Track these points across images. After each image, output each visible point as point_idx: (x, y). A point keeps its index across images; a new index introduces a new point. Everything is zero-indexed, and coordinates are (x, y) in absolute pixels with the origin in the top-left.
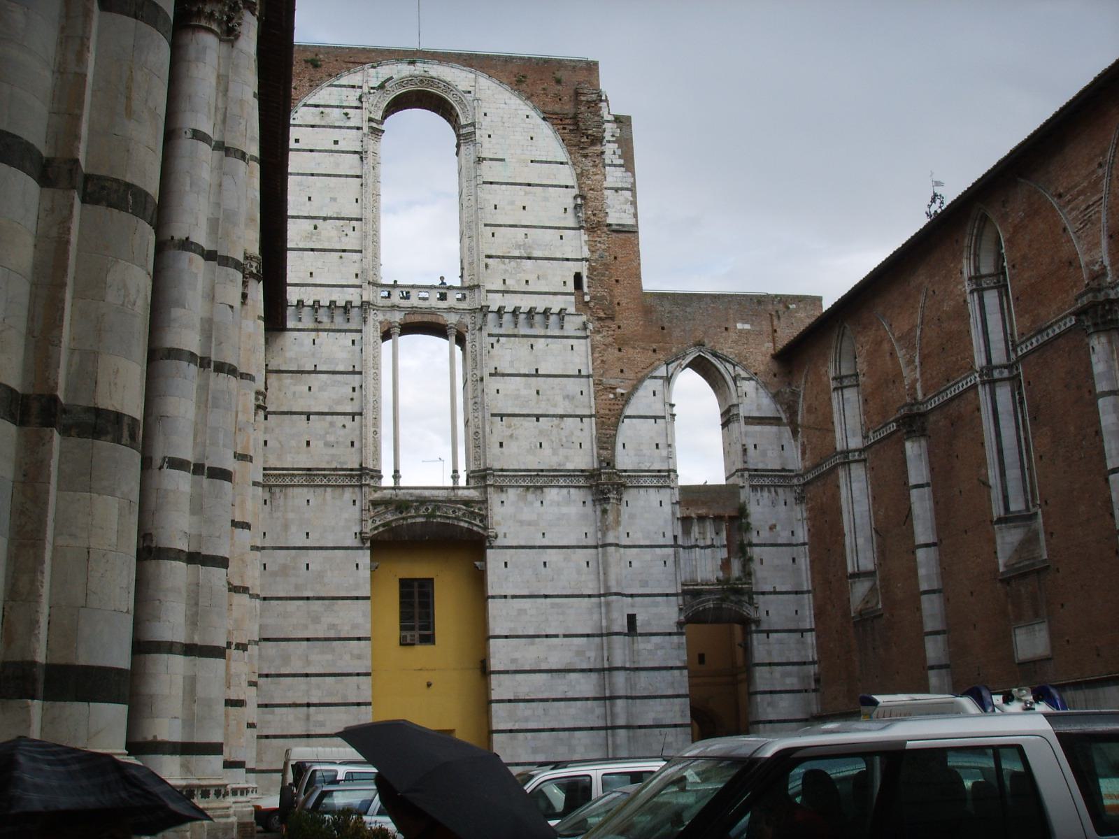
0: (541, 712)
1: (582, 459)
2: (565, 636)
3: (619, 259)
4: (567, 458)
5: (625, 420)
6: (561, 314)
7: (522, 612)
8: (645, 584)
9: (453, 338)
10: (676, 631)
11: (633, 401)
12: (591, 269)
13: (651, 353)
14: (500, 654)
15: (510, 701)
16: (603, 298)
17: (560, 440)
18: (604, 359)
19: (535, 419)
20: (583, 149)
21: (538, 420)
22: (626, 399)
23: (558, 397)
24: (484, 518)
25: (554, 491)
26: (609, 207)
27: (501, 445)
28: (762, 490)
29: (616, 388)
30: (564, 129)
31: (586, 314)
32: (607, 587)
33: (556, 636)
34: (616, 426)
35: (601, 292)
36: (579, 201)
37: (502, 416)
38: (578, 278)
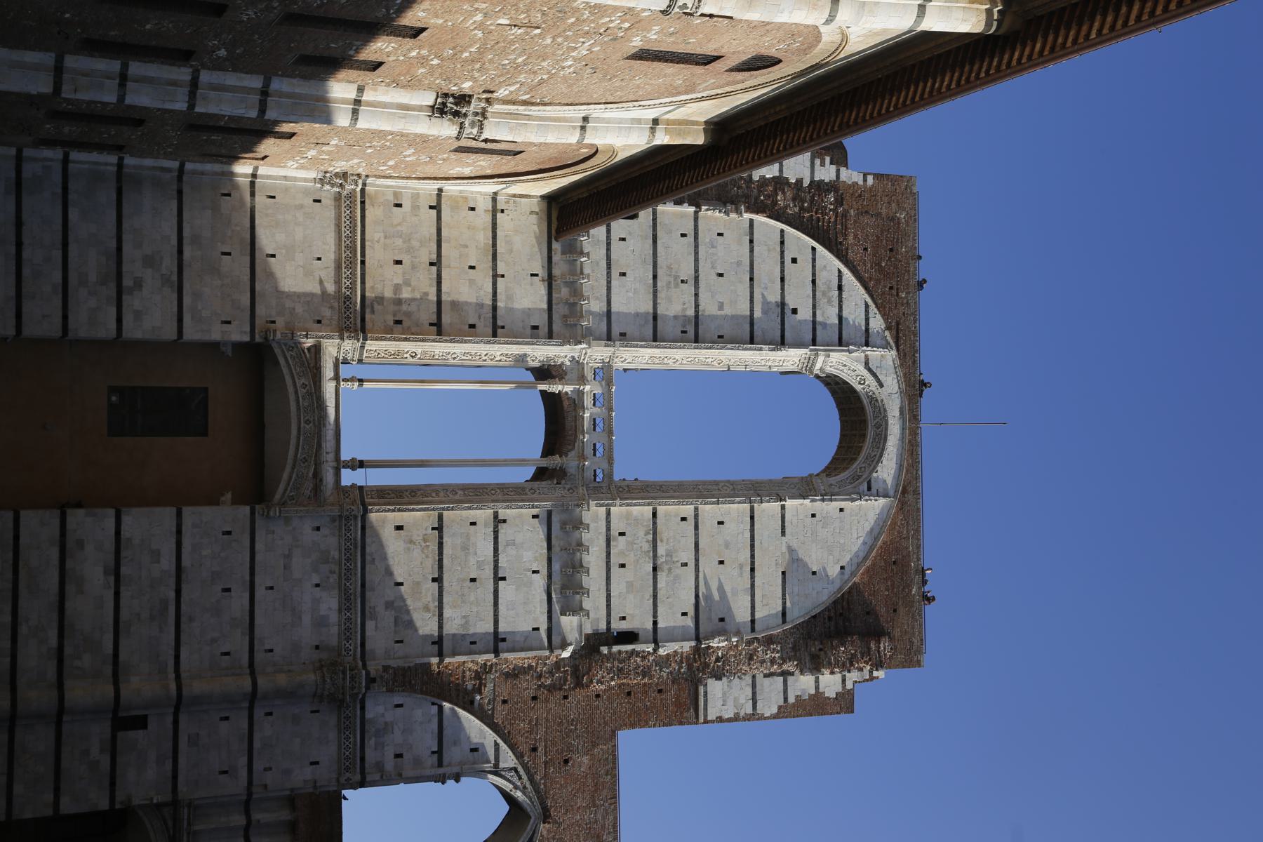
5: (437, 706)
9: (544, 463)
19: (436, 576)
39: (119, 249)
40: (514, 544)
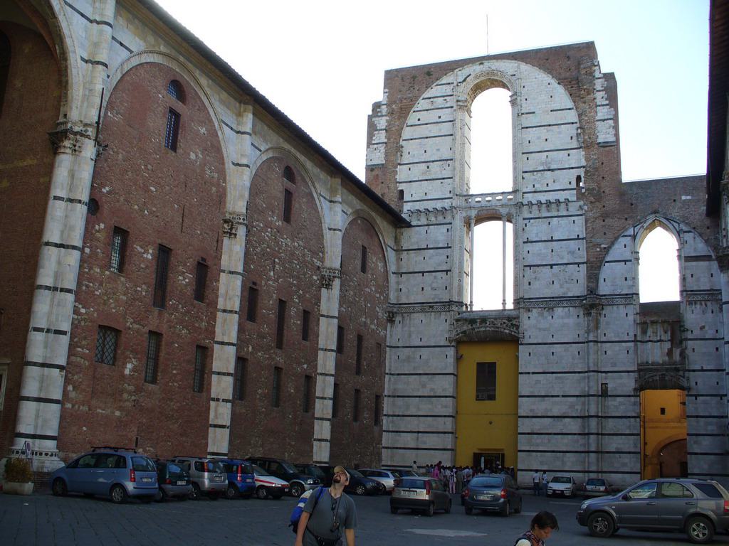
0: (546, 441)
1: (578, 289)
2: (563, 396)
3: (605, 164)
4: (568, 289)
6: (567, 201)
7: (538, 382)
8: (614, 365)
10: (633, 394)
11: (611, 252)
12: (586, 172)
13: (624, 221)
14: (525, 406)
15: (528, 434)
16: (593, 189)
17: (565, 278)
18: (594, 227)
20: (583, 98)
21: (552, 268)
22: (607, 250)
23: (563, 253)
24: (518, 327)
25: (560, 309)
26: (599, 132)
27: (530, 284)
28: (696, 304)
29: (600, 245)
30: (572, 87)
31: (583, 200)
32: (589, 367)
33: (558, 396)
34: (599, 268)
35: (593, 185)
36: (579, 131)
37: (530, 266)
38: (579, 179)
39: (420, 397)
40: (537, 234)
